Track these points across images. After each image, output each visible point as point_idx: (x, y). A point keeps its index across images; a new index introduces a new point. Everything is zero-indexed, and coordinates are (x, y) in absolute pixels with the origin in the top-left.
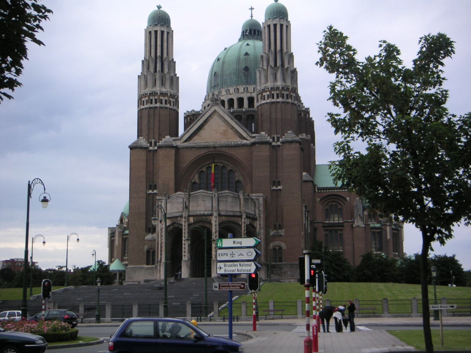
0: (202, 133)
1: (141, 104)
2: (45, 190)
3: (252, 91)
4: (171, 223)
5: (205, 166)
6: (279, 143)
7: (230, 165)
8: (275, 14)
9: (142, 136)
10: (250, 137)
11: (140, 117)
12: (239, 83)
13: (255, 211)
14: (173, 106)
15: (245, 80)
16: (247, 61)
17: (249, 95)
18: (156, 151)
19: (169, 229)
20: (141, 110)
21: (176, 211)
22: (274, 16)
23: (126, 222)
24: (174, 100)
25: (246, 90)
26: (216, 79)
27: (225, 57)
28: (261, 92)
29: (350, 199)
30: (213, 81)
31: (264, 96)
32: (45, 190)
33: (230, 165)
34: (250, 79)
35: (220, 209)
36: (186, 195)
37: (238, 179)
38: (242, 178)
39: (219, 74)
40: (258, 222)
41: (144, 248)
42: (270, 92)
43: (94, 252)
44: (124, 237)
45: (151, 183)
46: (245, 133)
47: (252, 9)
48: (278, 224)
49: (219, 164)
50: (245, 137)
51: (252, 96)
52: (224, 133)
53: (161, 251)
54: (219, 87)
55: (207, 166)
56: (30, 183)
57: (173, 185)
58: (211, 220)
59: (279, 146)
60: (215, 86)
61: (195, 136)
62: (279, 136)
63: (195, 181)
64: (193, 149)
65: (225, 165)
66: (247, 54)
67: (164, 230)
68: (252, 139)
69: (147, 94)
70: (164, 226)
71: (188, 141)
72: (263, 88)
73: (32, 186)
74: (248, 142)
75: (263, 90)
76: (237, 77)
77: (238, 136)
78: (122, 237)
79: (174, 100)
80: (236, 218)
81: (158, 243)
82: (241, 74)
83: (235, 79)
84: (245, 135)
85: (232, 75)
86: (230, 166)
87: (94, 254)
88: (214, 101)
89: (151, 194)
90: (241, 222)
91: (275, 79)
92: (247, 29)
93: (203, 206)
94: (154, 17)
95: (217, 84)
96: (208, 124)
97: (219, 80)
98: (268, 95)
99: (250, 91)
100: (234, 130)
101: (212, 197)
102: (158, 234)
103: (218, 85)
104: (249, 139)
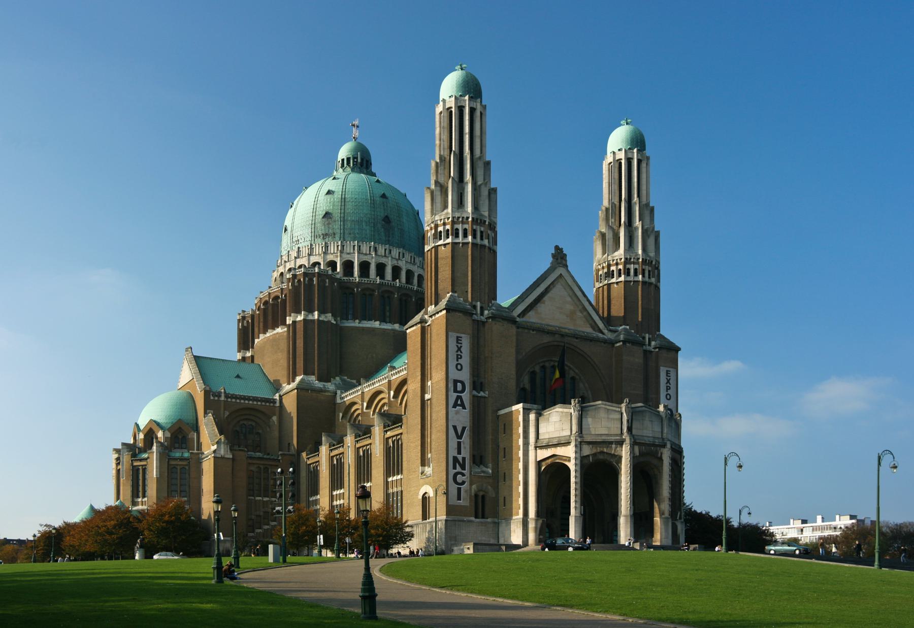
0: (541, 307)
9: (455, 292)
10: (607, 330)
17: (395, 262)
18: (484, 323)
19: (586, 461)
26: (329, 224)
30: (318, 225)
34: (393, 237)
35: (663, 437)
37: (583, 393)
39: (337, 215)
52: (572, 315)
55: (541, 365)
58: (662, 454)
59: (651, 352)
60: (325, 236)
61: (529, 311)
64: (531, 332)
66: (384, 196)
68: (610, 333)
71: (521, 316)
78: (168, 462)
82: (379, 226)
84: (601, 325)
85: (364, 224)
86: (573, 370)
88: (559, 258)
89: (478, 397)
95: (331, 231)
96: (549, 295)
97: (337, 227)
103: (334, 234)
104: (606, 334)
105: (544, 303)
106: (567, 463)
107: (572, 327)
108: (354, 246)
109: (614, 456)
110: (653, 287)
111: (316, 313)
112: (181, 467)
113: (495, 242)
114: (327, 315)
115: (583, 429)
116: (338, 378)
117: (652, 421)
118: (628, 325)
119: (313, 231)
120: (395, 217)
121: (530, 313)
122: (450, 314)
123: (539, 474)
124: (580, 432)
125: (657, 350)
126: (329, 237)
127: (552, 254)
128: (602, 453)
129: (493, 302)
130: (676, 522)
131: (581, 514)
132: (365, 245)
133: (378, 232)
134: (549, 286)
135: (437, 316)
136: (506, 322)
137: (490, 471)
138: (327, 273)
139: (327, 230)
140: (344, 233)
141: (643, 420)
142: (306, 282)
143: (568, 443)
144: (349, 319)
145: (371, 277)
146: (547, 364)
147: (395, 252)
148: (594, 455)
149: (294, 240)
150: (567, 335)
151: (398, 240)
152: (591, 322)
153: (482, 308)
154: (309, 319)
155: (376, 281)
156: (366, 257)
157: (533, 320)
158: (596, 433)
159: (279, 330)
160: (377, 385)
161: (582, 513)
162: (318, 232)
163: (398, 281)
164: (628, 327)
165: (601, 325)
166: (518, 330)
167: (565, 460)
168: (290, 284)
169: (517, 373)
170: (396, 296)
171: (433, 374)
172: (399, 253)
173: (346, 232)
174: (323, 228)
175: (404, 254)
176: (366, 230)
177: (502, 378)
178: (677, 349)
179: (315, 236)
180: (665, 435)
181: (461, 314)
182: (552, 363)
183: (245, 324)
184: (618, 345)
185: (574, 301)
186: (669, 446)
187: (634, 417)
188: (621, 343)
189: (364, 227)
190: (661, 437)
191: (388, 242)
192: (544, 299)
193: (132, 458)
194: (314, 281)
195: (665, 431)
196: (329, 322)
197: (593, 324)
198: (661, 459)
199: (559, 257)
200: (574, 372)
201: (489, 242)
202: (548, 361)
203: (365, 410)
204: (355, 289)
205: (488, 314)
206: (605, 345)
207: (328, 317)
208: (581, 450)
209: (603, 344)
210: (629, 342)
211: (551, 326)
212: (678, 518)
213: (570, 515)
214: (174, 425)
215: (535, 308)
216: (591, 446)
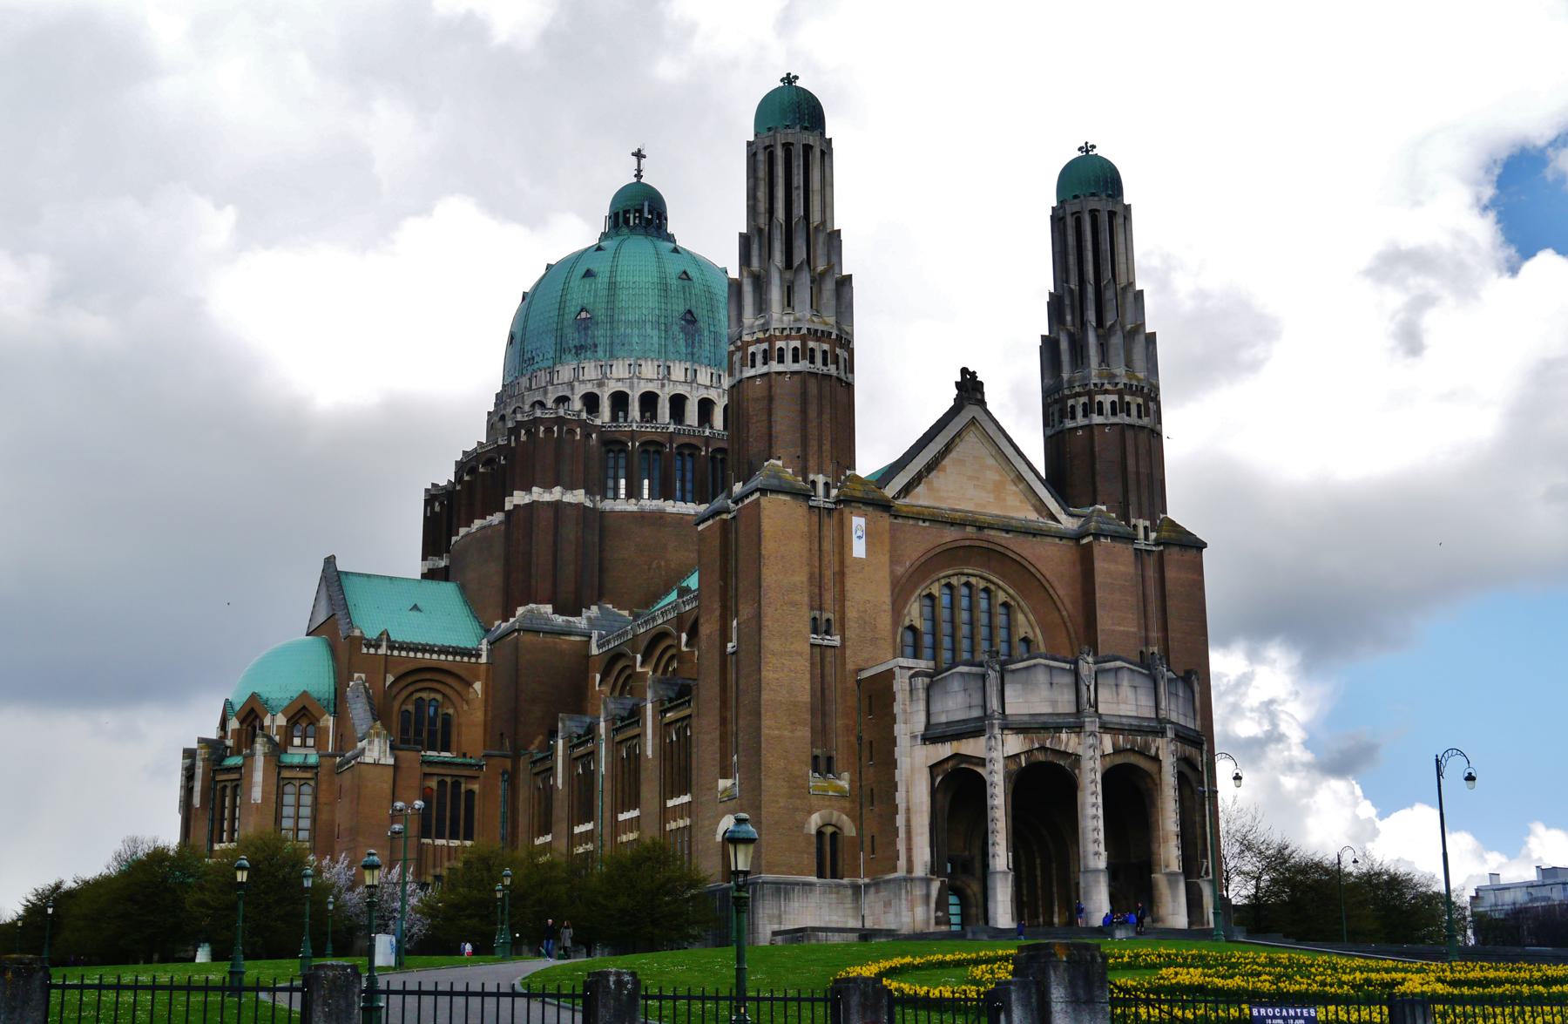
5: (938, 580)
7: (1006, 587)
9: (779, 458)
17: (704, 394)
19: (1013, 767)
20: (774, 376)
21: (1047, 709)
22: (1107, 190)
23: (279, 727)
25: (692, 381)
31: (1100, 403)
33: (1006, 587)
34: (701, 347)
35: (1160, 717)
38: (1038, 631)
41: (809, 823)
42: (1120, 394)
45: (817, 614)
46: (1053, 499)
47: (639, 155)
49: (973, 580)
50: (1054, 512)
51: (709, 397)
54: (600, 354)
55: (943, 582)
58: (1158, 749)
61: (917, 485)
62: (1148, 523)
63: (913, 623)
64: (921, 523)
65: (992, 587)
66: (685, 276)
69: (799, 329)
75: (1095, 385)
78: (279, 773)
82: (676, 328)
83: (655, 339)
85: (648, 326)
88: (970, 389)
90: (1200, 764)
91: (1129, 364)
92: (637, 207)
93: (1134, 703)
96: (953, 455)
103: (596, 346)
105: (944, 470)
106: (980, 770)
109: (1065, 754)
110: (1143, 436)
111: (557, 490)
113: (850, 367)
114: (575, 492)
115: (1006, 705)
116: (594, 608)
117: (1135, 687)
118: (1103, 504)
119: (558, 341)
120: (705, 312)
123: (934, 792)
124: (1001, 711)
125: (1161, 548)
126: (586, 351)
127: (957, 383)
128: (1043, 748)
129: (848, 472)
131: (1008, 868)
133: (673, 339)
134: (953, 439)
135: (747, 501)
136: (871, 509)
137: (847, 786)
138: (579, 416)
139: (583, 340)
140: (612, 344)
141: (1117, 685)
142: (541, 435)
143: (977, 732)
144: (617, 498)
145: (659, 422)
146: (954, 581)
147: (704, 374)
148: (1029, 752)
149: (525, 358)
150: (991, 527)
151: (710, 352)
153: (826, 484)
154: (544, 500)
155: (668, 428)
156: (650, 385)
157: (921, 502)
158: (1031, 712)
159: (497, 518)
160: (660, 621)
161: (1011, 866)
162: (567, 343)
163: (707, 425)
164: (1104, 508)
165: (1053, 505)
166: (896, 521)
167: (977, 764)
168: (513, 438)
169: (894, 603)
170: (703, 453)
171: (741, 607)
172: (712, 374)
173: (617, 341)
174: (576, 335)
175: (720, 376)
176: (652, 337)
177: (866, 611)
178: (1200, 546)
180: (1163, 714)
181: (787, 498)
182: (964, 579)
183: (437, 508)
184: (1085, 541)
185: (1000, 464)
186: (1170, 734)
187: (1099, 681)
188: (1091, 538)
189: (649, 331)
190: (1153, 716)
191: (692, 357)
192: (944, 463)
193: (214, 765)
194: (554, 431)
195: (1163, 704)
196: (579, 506)
197: (1038, 503)
198: (1156, 759)
199: (970, 388)
200: (1008, 594)
201: (837, 369)
202: (953, 575)
203: (639, 669)
204: (630, 444)
205: (837, 496)
206: (1061, 543)
207: (578, 496)
208: (1003, 745)
209: (1057, 540)
210: (1106, 536)
211: (957, 511)
214: (294, 702)
216: (1021, 736)
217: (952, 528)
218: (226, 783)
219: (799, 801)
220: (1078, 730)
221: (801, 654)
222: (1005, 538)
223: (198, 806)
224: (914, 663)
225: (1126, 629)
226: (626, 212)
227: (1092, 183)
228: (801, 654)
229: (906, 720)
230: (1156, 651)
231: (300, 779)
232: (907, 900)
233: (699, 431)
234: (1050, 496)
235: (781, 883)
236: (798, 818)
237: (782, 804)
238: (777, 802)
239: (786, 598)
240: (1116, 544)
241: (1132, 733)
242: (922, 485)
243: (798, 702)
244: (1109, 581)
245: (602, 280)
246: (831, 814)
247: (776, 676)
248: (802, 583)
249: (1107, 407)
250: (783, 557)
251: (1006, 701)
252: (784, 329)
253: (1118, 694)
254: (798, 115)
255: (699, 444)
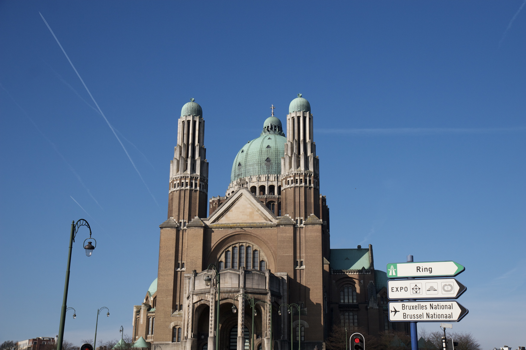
0: (229, 214)
1: (172, 187)
2: (91, 234)
3: (274, 180)
4: (198, 300)
6: (302, 225)
8: (299, 107)
11: (172, 199)
12: (261, 173)
13: (279, 289)
14: (203, 189)
15: (267, 170)
16: (268, 152)
17: (270, 183)
19: (196, 306)
22: (298, 109)
23: (152, 301)
24: (204, 184)
25: (268, 179)
26: (240, 169)
27: (248, 150)
28: (286, 177)
29: (364, 282)
31: (288, 181)
32: (91, 234)
34: (272, 169)
36: (214, 272)
40: (282, 300)
41: (170, 325)
43: (122, 328)
44: (149, 315)
46: (270, 215)
48: (301, 303)
49: (244, 244)
50: (270, 219)
52: (251, 214)
53: (188, 328)
56: (75, 224)
57: (201, 264)
60: (239, 175)
61: (222, 217)
62: (302, 218)
64: (220, 229)
65: (250, 245)
67: (191, 306)
70: (191, 303)
71: (216, 221)
72: (287, 174)
73: (76, 228)
74: (273, 223)
75: (287, 175)
76: (259, 167)
77: (264, 218)
78: (147, 315)
79: (204, 184)
80: (261, 296)
81: (184, 320)
82: (263, 164)
83: (257, 169)
85: (255, 165)
87: (122, 330)
91: (298, 166)
92: (268, 125)
93: (231, 283)
94: (187, 108)
95: (241, 173)
98: (292, 180)
99: (271, 180)
100: (260, 212)
101: (239, 275)
102: (185, 311)
103: (242, 174)
105: (232, 211)
107: (250, 222)
108: (257, 177)
112: (153, 317)
118: (288, 214)
120: (274, 157)
121: (222, 218)
122: (162, 230)
124: (193, 289)
130: (264, 339)
132: (254, 177)
136: (197, 228)
141: (224, 278)
152: (264, 216)
164: (288, 215)
165: (270, 216)
173: (247, 171)
174: (238, 171)
177: (193, 260)
179: (235, 177)
182: (241, 244)
185: (252, 206)
190: (238, 287)
192: (232, 209)
197: (265, 217)
198: (237, 300)
209: (270, 228)
210: (282, 225)
212: (265, 336)
213: (208, 336)
215: (225, 215)
216: (197, 296)
217: (231, 229)
218: (151, 317)
219: (167, 319)
220: (210, 293)
221: (171, 275)
222: (251, 230)
223: (133, 325)
224: (189, 275)
225: (288, 254)
226: (275, 127)
227: (294, 108)
228: (171, 275)
229: (186, 293)
230: (303, 261)
231: (153, 316)
232: (181, 348)
233: (263, 197)
234: (269, 214)
235: (159, 344)
236: (167, 324)
237: (162, 320)
238: (160, 320)
239: (167, 258)
240: (286, 227)
241: (228, 293)
242: (223, 217)
243: (169, 289)
244: (283, 239)
245: (245, 152)
246: (178, 322)
247: (162, 282)
248: (173, 253)
249: (290, 182)
250: (167, 246)
251: (195, 286)
252: (175, 178)
253: (224, 281)
254: (187, 112)
255: (263, 201)
